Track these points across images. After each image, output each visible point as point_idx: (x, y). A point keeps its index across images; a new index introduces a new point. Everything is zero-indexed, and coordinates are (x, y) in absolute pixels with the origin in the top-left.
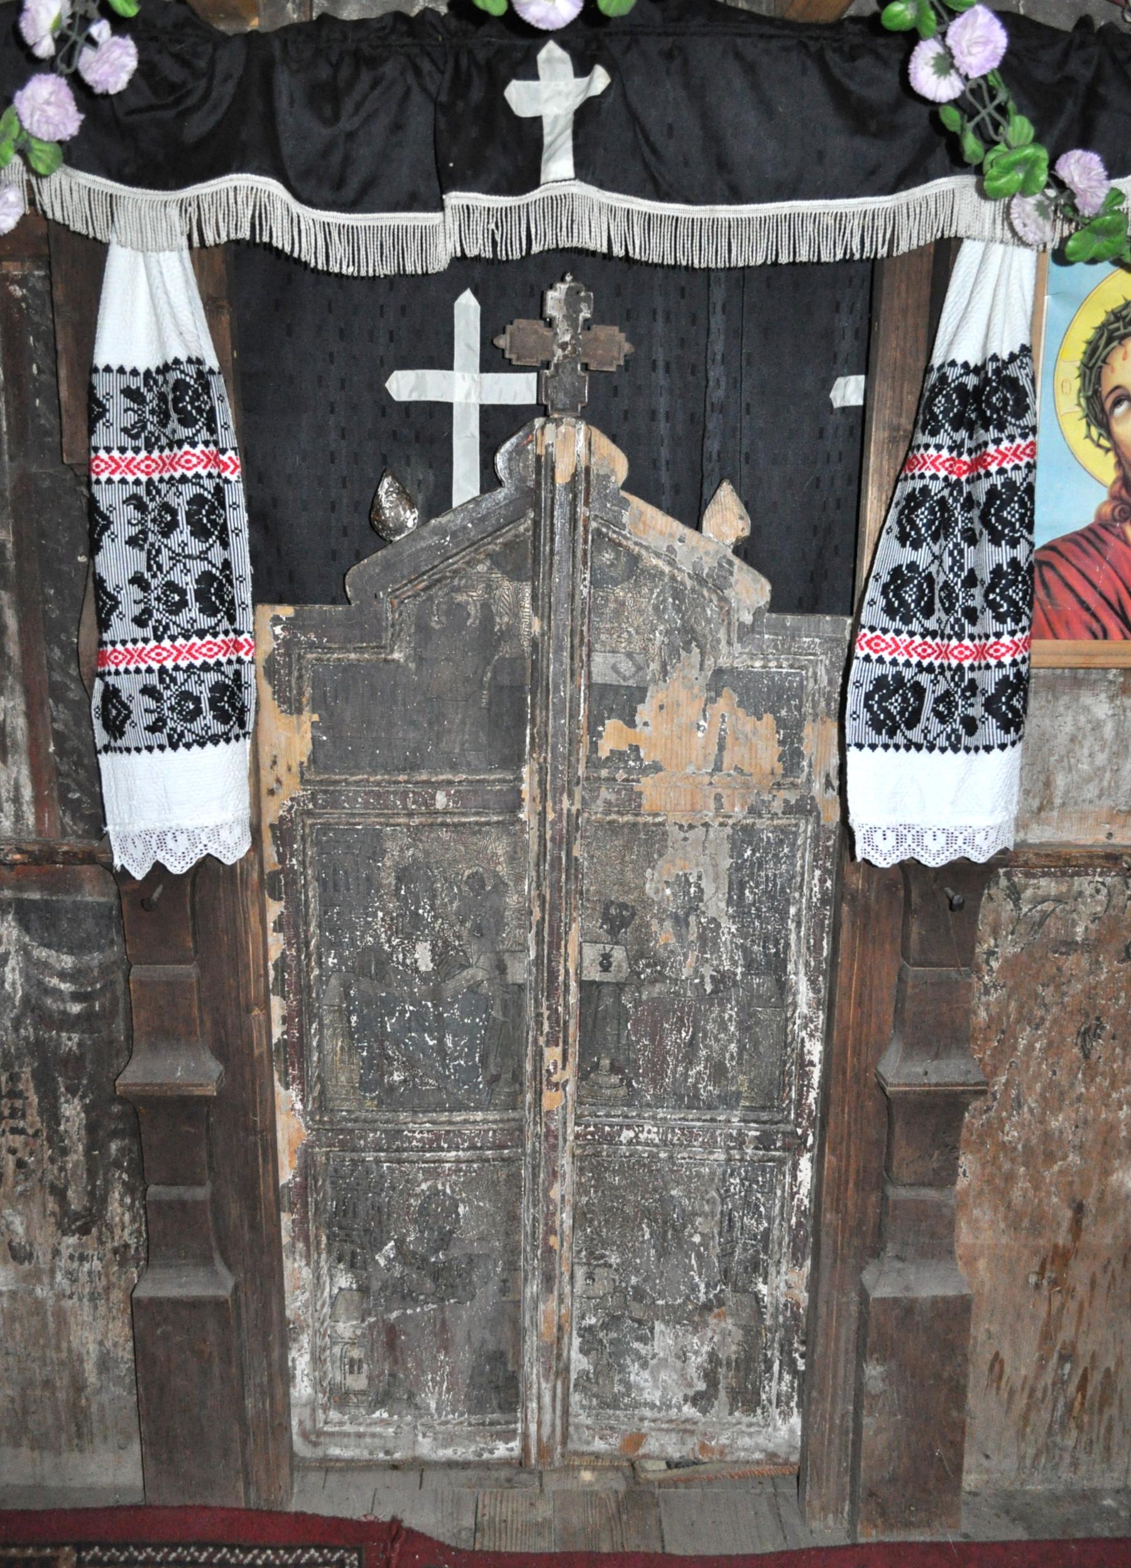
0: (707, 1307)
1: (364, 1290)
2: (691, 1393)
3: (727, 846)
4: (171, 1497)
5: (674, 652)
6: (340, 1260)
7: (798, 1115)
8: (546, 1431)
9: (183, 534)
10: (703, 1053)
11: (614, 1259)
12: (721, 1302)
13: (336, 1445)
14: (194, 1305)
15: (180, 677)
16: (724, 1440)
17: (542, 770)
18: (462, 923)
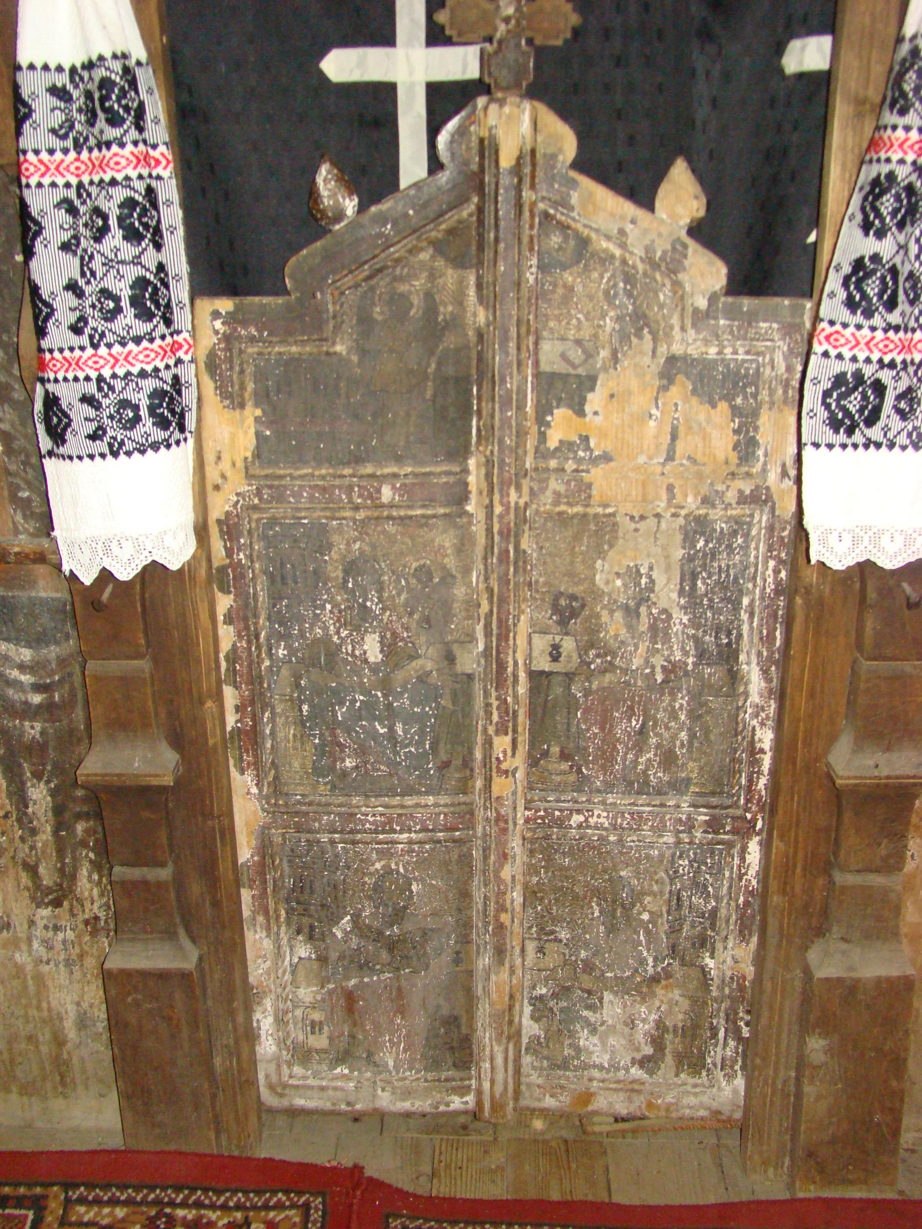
0: (655, 979)
1: (323, 959)
2: (638, 1056)
3: (679, 537)
4: (147, 1143)
5: (624, 338)
6: (299, 932)
7: (748, 801)
8: (499, 1089)
9: (115, 238)
10: (653, 741)
11: (564, 935)
12: (668, 976)
13: (300, 1097)
14: (163, 976)
15: (118, 384)
16: (669, 1099)
17: (489, 463)
18: (411, 614)
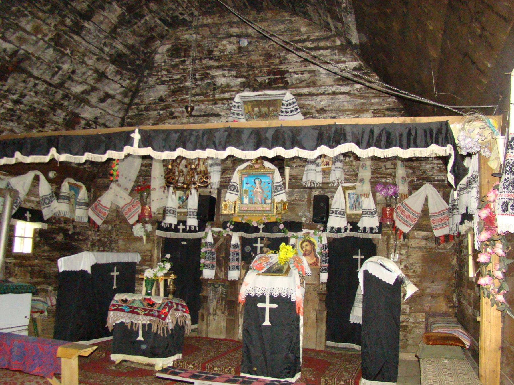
14: (232, 320)
